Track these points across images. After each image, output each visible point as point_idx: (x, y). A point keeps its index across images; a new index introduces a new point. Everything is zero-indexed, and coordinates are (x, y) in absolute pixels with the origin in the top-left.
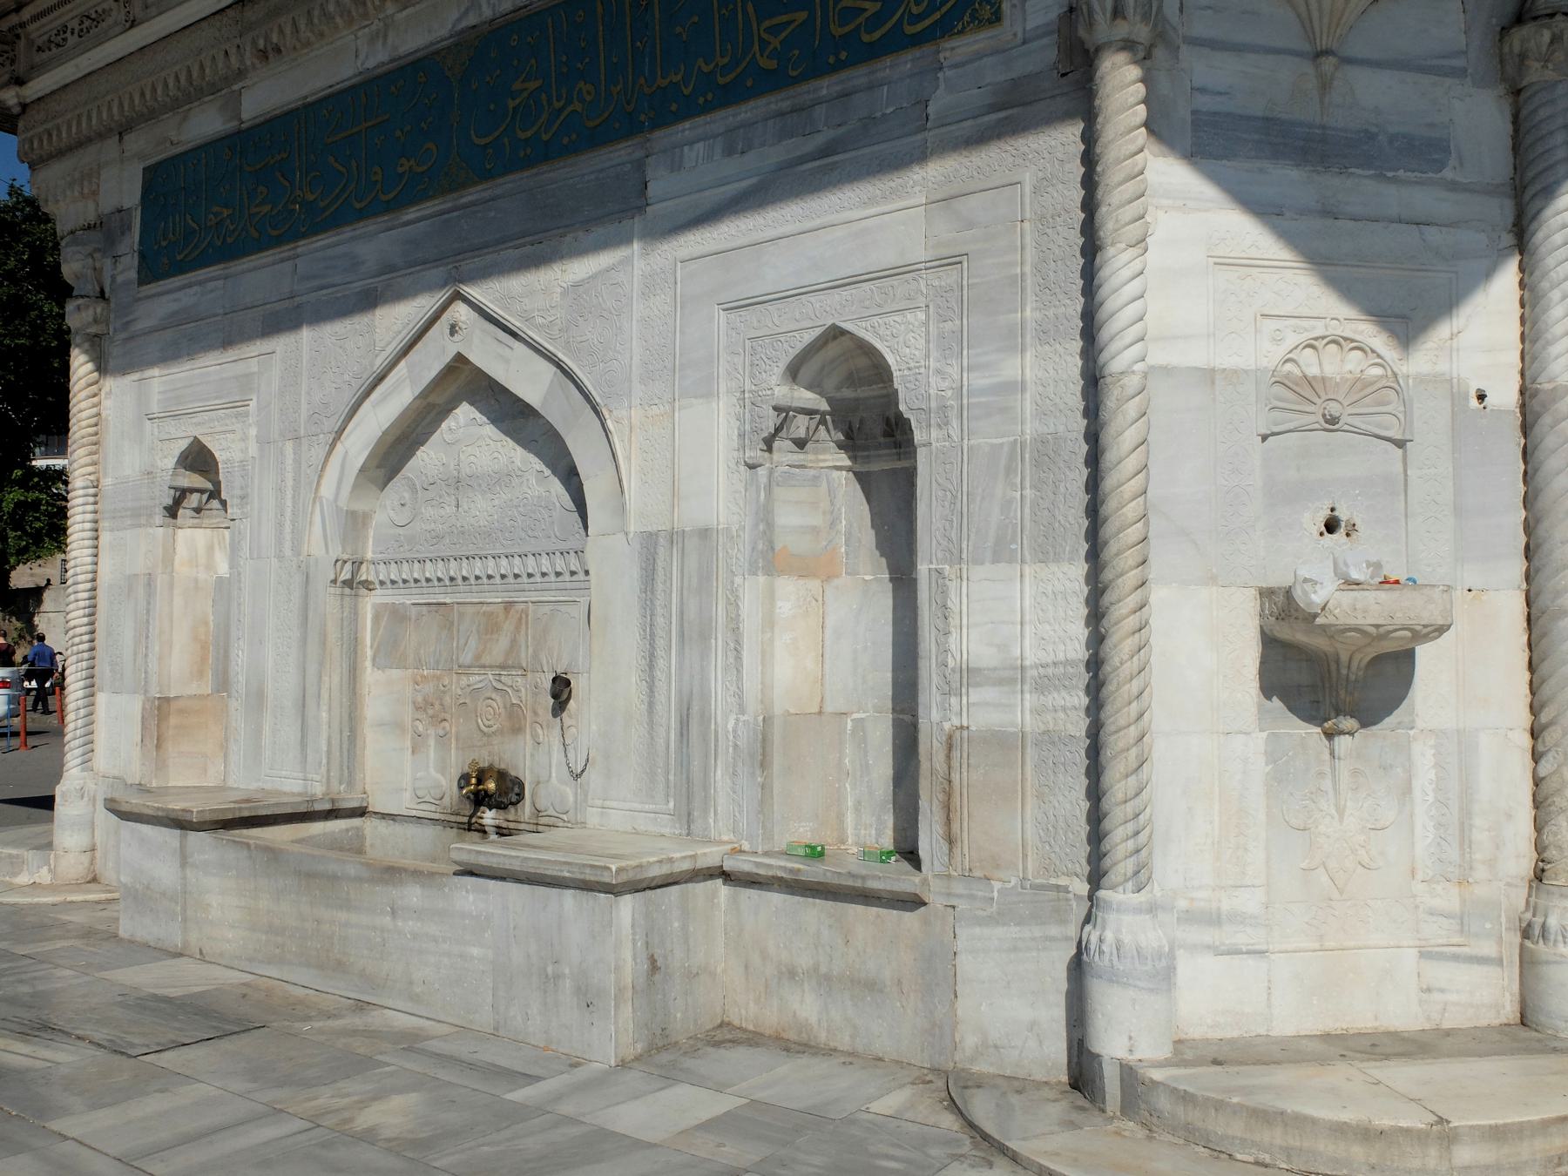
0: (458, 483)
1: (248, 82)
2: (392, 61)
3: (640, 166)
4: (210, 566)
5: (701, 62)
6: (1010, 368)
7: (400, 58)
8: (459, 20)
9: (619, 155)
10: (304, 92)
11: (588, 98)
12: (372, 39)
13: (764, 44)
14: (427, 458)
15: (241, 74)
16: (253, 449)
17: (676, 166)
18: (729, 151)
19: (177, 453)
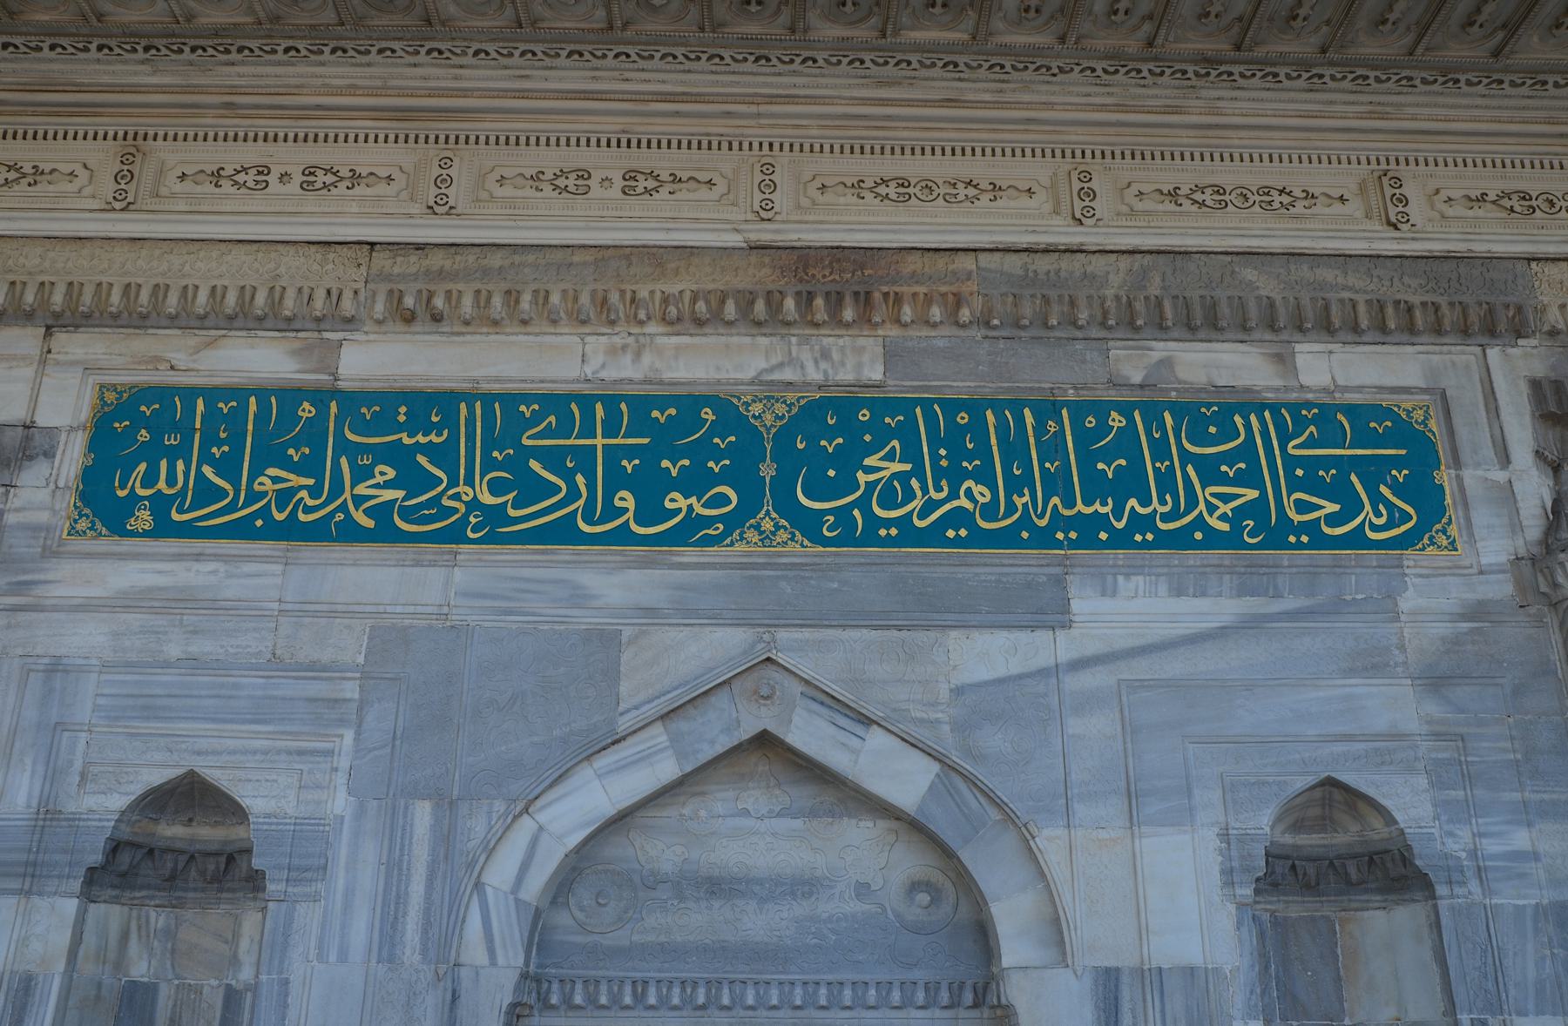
0: (718, 887)
1: (357, 336)
2: (647, 381)
3: (1060, 583)
4: (120, 965)
5: (1133, 502)
6: (1521, 839)
7: (661, 382)
8: (772, 369)
9: (1025, 564)
10: (476, 373)
11: (982, 500)
12: (613, 351)
13: (1211, 508)
14: (659, 850)
15: (350, 322)
16: (340, 803)
17: (1109, 591)
18: (1178, 591)
19: (137, 789)
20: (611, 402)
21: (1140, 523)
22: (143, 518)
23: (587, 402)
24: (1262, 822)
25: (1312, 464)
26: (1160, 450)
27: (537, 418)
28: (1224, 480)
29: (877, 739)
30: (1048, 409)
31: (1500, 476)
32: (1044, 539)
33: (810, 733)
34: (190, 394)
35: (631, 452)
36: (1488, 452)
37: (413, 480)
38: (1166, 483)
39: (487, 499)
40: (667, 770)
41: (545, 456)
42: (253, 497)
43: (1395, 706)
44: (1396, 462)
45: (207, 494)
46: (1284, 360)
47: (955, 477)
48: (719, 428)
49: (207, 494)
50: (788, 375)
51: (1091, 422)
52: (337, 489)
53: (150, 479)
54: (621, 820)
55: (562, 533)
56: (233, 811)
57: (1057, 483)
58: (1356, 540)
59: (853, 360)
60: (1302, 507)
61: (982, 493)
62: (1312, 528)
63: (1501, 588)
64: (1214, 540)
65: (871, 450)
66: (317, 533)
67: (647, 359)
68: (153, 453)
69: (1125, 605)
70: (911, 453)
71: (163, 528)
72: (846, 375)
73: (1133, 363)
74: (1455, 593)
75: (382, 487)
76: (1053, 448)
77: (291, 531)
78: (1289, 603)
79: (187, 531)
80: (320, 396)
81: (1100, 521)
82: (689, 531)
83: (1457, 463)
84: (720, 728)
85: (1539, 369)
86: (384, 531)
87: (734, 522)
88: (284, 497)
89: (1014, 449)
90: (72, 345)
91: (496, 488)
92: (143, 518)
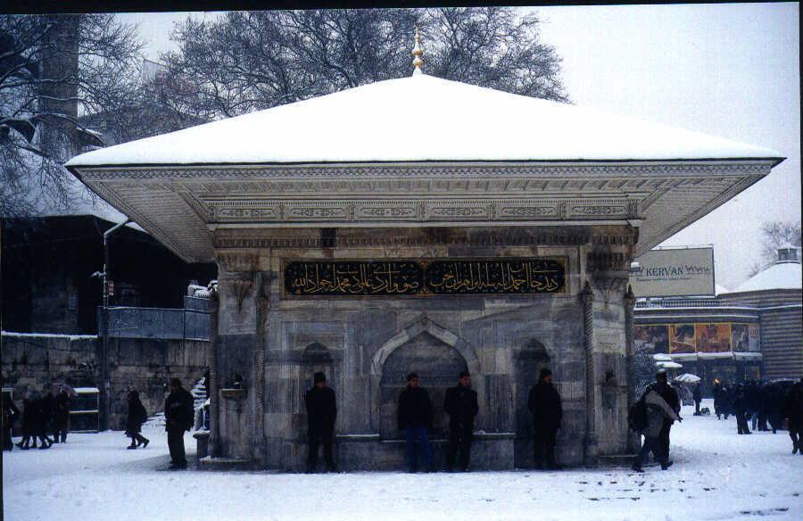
0: (417, 359)
20: (392, 263)
21: (501, 288)
22: (299, 291)
23: (386, 263)
24: (519, 348)
25: (538, 274)
26: (506, 272)
27: (377, 267)
28: (518, 278)
29: (447, 332)
30: (482, 263)
31: (578, 276)
32: (480, 292)
33: (433, 331)
34: (303, 263)
35: (396, 274)
36: (576, 270)
37: (352, 282)
38: (506, 278)
39: (368, 286)
40: (406, 338)
41: (380, 276)
42: (320, 286)
43: (549, 325)
44: (556, 274)
45: (311, 286)
46: (534, 250)
47: (463, 279)
48: (414, 269)
49: (311, 286)
50: (428, 256)
51: (491, 266)
52: (337, 284)
53: (299, 283)
54: (398, 349)
55: (384, 292)
56: (325, 348)
57: (484, 280)
58: (545, 291)
59: (442, 252)
60: (534, 284)
61: (468, 282)
62: (536, 289)
63: (573, 301)
64: (515, 291)
65: (445, 273)
66: (335, 293)
67: (398, 253)
68: (298, 277)
69: (493, 306)
70: (454, 274)
71: (303, 293)
72: (440, 256)
73: (501, 252)
74: (565, 301)
75: (346, 283)
76: (483, 271)
77: (329, 293)
78: (529, 304)
79: (308, 294)
80: (331, 264)
81: (492, 288)
82: (409, 292)
83: (569, 274)
84: (414, 331)
85: (590, 250)
86: (348, 293)
87: (420, 288)
88: (327, 286)
89: (476, 273)
90: (276, 252)
91: (369, 284)
92: (299, 291)
